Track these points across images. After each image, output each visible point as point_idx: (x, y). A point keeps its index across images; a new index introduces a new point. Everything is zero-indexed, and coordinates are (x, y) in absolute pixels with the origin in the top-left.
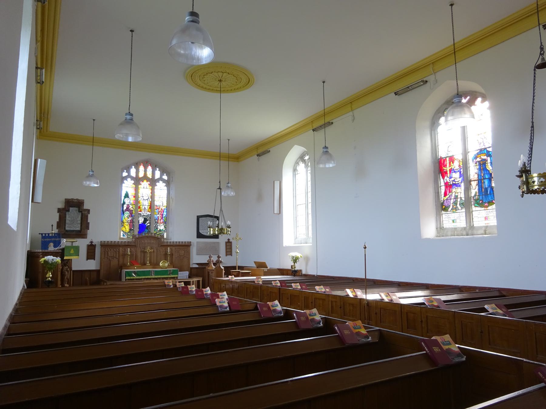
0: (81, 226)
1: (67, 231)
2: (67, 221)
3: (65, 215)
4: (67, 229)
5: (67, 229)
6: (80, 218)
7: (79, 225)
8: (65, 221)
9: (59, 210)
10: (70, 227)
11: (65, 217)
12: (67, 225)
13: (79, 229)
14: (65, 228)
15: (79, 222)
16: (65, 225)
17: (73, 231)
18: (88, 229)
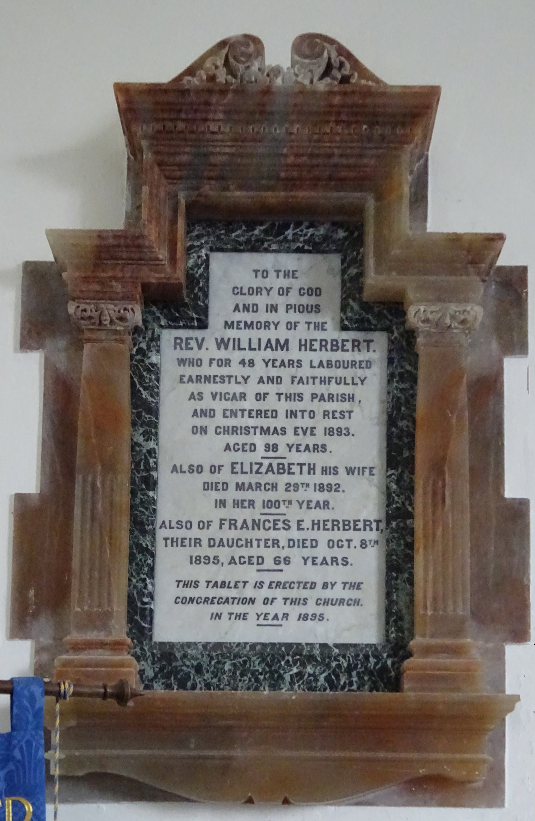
0: (398, 567)
1: (169, 662)
2: (176, 499)
3: (144, 376)
4: (175, 624)
5: (175, 624)
6: (365, 441)
7: (367, 564)
8: (144, 480)
9: (50, 305)
10: (222, 598)
11: (145, 414)
12: (171, 566)
13: (359, 625)
14: (140, 616)
15: (364, 499)
16: (142, 560)
17: (273, 661)
18: (520, 634)
